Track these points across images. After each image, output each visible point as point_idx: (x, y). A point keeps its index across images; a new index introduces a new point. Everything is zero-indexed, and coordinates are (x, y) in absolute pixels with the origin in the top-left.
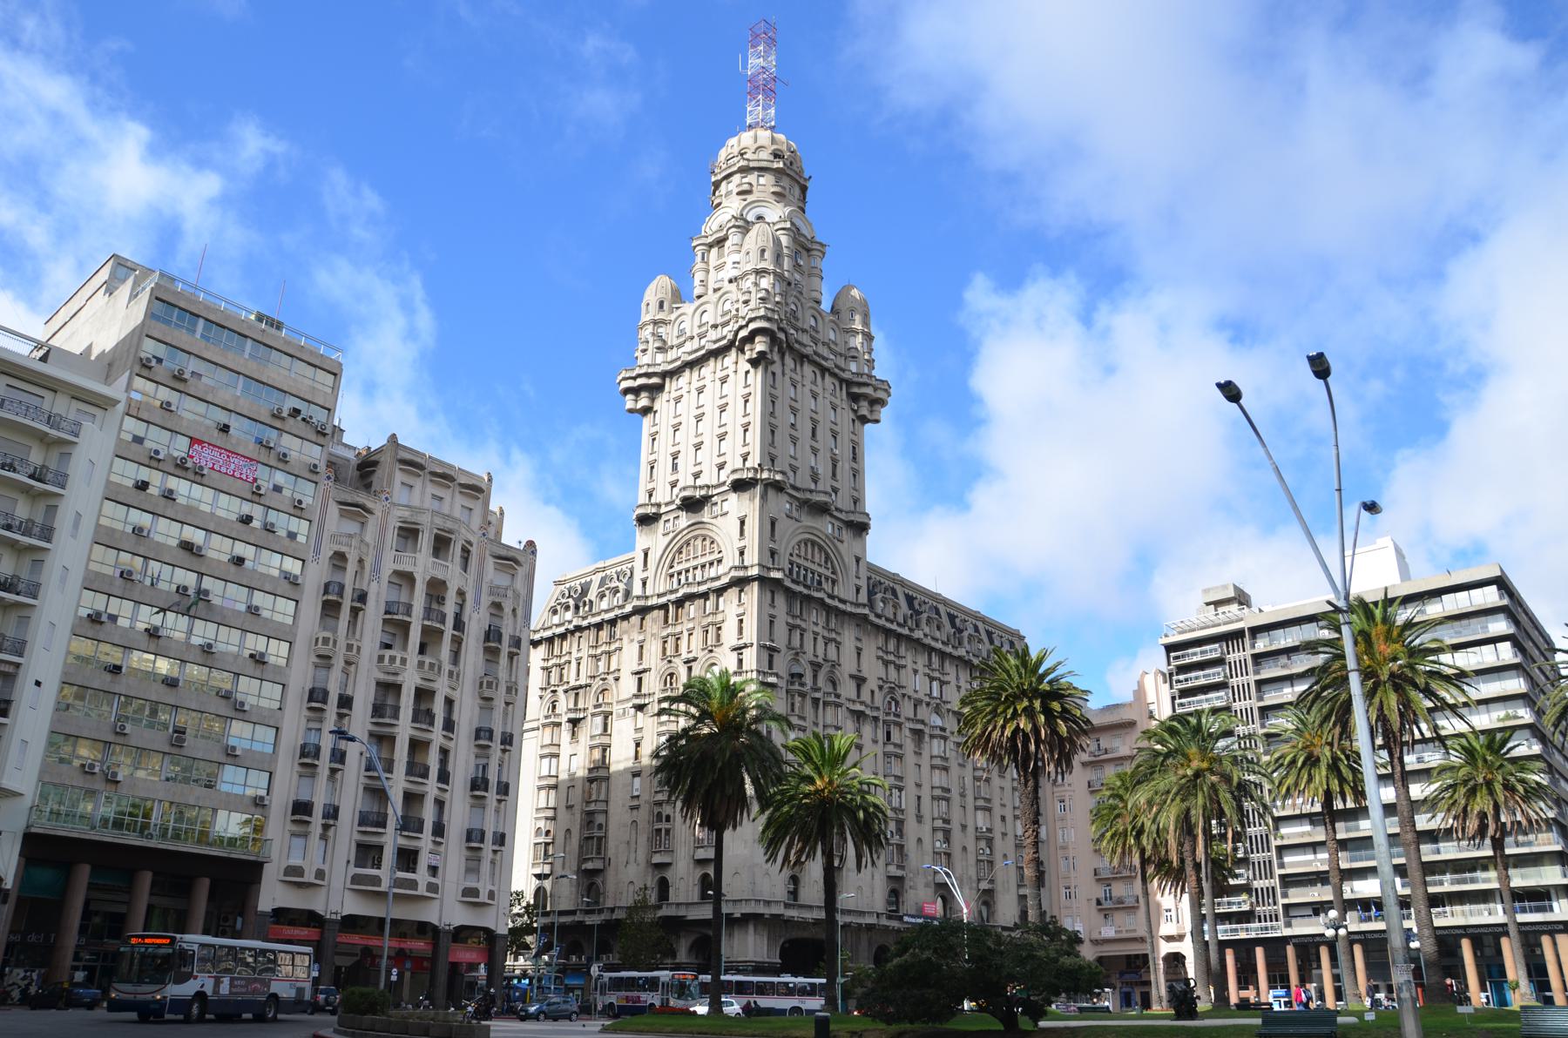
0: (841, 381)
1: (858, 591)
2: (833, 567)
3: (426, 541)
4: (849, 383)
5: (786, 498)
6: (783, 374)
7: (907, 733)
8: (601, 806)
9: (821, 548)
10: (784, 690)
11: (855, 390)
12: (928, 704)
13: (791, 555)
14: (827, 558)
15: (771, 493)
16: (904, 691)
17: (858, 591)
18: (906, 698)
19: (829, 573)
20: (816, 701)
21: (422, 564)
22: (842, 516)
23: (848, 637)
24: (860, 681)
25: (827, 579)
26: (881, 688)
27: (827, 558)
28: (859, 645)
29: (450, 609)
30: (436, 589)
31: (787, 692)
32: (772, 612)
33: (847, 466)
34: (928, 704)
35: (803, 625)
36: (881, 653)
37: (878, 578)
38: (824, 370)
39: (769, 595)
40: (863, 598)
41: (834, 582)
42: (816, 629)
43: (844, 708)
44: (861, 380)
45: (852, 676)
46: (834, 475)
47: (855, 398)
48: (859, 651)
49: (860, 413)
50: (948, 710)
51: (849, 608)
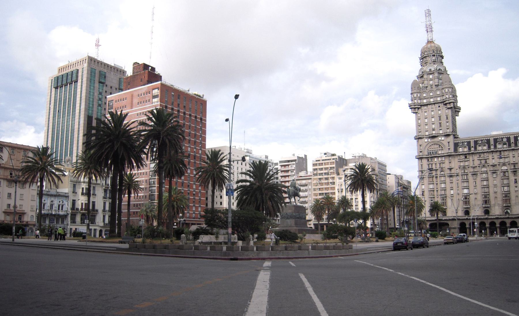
0: (441, 103)
2: (441, 146)
4: (443, 102)
5: (425, 138)
6: (422, 112)
7: (470, 175)
8: (488, 193)
9: (437, 144)
10: (427, 178)
11: (444, 103)
12: (479, 166)
14: (440, 145)
15: (419, 140)
16: (469, 166)
17: (449, 149)
18: (470, 167)
20: (436, 177)
22: (444, 134)
23: (447, 161)
24: (450, 169)
26: (459, 168)
27: (440, 145)
28: (450, 161)
31: (428, 177)
32: (422, 164)
33: (445, 122)
34: (479, 166)
35: (432, 163)
36: (459, 160)
38: (434, 104)
39: (420, 161)
40: (452, 150)
42: (436, 162)
43: (446, 176)
44: (445, 100)
45: (448, 169)
46: (440, 126)
47: (446, 104)
48: (450, 162)
49: (448, 107)
50: (489, 166)
51: (445, 155)
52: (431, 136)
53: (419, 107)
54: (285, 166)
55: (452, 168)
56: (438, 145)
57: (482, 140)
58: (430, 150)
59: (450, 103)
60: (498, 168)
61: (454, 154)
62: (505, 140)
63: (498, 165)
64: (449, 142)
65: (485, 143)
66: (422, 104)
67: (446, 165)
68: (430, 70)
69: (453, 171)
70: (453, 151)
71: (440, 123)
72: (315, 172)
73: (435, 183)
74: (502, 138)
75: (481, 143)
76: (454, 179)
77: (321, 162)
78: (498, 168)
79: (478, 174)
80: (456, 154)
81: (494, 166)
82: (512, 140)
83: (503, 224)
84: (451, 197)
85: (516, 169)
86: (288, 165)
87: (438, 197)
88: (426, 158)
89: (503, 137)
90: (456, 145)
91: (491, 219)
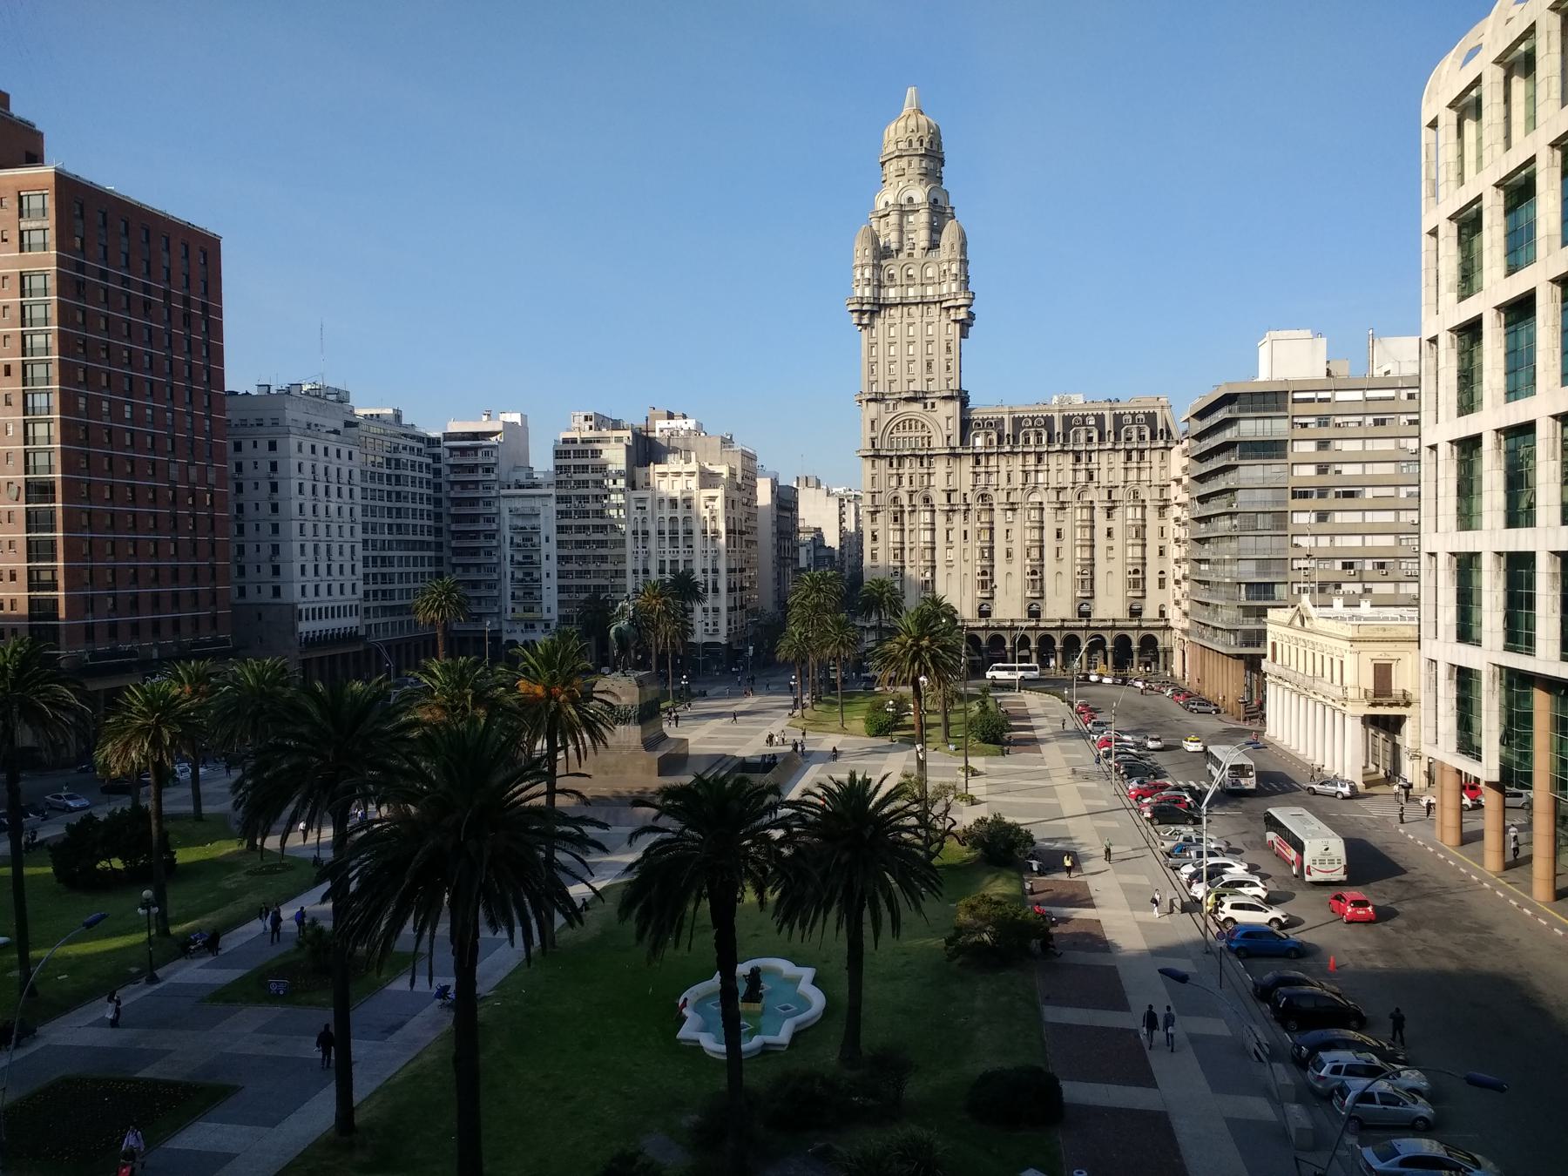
0: (935, 303)
1: (948, 438)
3: (666, 504)
4: (941, 302)
11: (944, 305)
13: (891, 433)
17: (948, 438)
19: (925, 434)
21: (667, 513)
25: (923, 438)
27: (923, 426)
29: (681, 528)
30: (673, 520)
33: (942, 360)
37: (981, 417)
40: (955, 441)
41: (929, 437)
48: (949, 474)
49: (952, 318)
52: (904, 395)
53: (876, 308)
54: (463, 450)
55: (955, 490)
56: (920, 425)
57: (1033, 419)
58: (899, 435)
59: (958, 307)
60: (1067, 496)
61: (958, 451)
62: (1092, 422)
63: (1069, 489)
64: (948, 418)
65: (1042, 427)
66: (881, 301)
67: (939, 481)
68: (910, 199)
69: (956, 498)
70: (958, 445)
71: (929, 365)
72: (563, 477)
73: (907, 527)
74: (1084, 417)
75: (1029, 427)
76: (957, 518)
77: (579, 446)
78: (1067, 496)
79: (1019, 511)
80: (965, 451)
81: (1059, 490)
82: (1109, 426)
83: (1072, 643)
84: (947, 566)
85: (1114, 501)
86: (475, 449)
87: (912, 567)
88: (885, 457)
89: (1085, 413)
90: (966, 425)
91: (1045, 629)
